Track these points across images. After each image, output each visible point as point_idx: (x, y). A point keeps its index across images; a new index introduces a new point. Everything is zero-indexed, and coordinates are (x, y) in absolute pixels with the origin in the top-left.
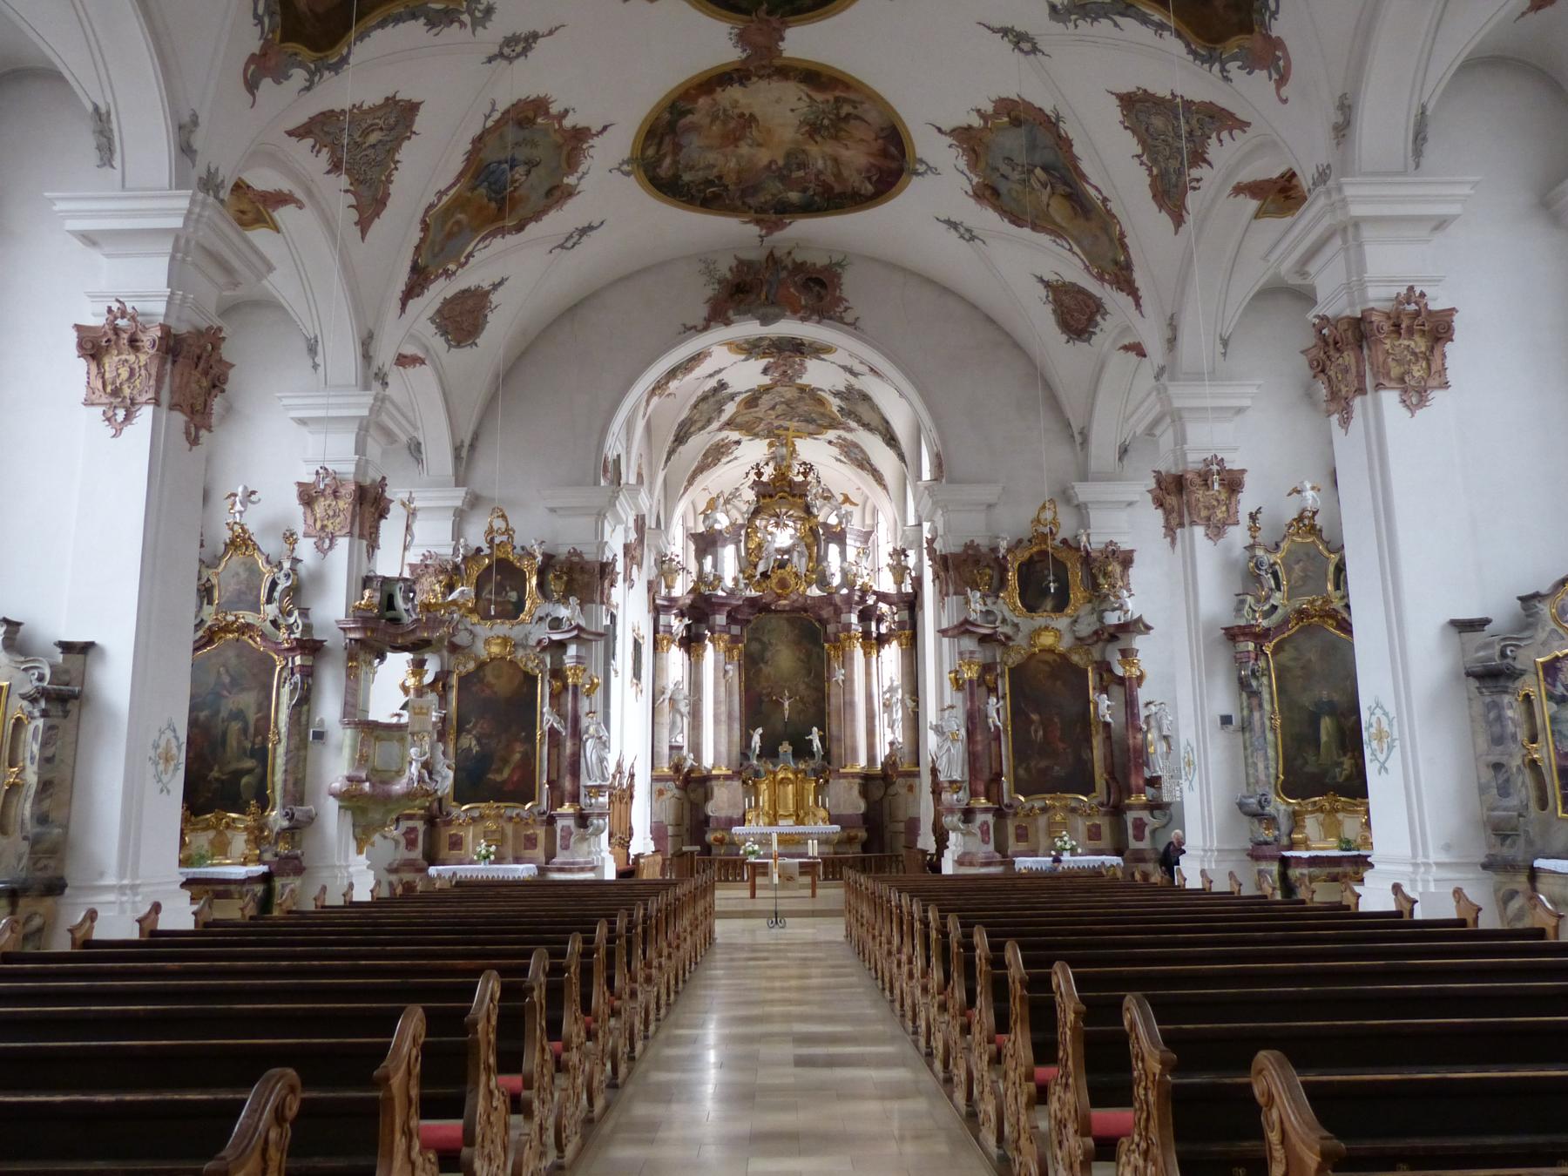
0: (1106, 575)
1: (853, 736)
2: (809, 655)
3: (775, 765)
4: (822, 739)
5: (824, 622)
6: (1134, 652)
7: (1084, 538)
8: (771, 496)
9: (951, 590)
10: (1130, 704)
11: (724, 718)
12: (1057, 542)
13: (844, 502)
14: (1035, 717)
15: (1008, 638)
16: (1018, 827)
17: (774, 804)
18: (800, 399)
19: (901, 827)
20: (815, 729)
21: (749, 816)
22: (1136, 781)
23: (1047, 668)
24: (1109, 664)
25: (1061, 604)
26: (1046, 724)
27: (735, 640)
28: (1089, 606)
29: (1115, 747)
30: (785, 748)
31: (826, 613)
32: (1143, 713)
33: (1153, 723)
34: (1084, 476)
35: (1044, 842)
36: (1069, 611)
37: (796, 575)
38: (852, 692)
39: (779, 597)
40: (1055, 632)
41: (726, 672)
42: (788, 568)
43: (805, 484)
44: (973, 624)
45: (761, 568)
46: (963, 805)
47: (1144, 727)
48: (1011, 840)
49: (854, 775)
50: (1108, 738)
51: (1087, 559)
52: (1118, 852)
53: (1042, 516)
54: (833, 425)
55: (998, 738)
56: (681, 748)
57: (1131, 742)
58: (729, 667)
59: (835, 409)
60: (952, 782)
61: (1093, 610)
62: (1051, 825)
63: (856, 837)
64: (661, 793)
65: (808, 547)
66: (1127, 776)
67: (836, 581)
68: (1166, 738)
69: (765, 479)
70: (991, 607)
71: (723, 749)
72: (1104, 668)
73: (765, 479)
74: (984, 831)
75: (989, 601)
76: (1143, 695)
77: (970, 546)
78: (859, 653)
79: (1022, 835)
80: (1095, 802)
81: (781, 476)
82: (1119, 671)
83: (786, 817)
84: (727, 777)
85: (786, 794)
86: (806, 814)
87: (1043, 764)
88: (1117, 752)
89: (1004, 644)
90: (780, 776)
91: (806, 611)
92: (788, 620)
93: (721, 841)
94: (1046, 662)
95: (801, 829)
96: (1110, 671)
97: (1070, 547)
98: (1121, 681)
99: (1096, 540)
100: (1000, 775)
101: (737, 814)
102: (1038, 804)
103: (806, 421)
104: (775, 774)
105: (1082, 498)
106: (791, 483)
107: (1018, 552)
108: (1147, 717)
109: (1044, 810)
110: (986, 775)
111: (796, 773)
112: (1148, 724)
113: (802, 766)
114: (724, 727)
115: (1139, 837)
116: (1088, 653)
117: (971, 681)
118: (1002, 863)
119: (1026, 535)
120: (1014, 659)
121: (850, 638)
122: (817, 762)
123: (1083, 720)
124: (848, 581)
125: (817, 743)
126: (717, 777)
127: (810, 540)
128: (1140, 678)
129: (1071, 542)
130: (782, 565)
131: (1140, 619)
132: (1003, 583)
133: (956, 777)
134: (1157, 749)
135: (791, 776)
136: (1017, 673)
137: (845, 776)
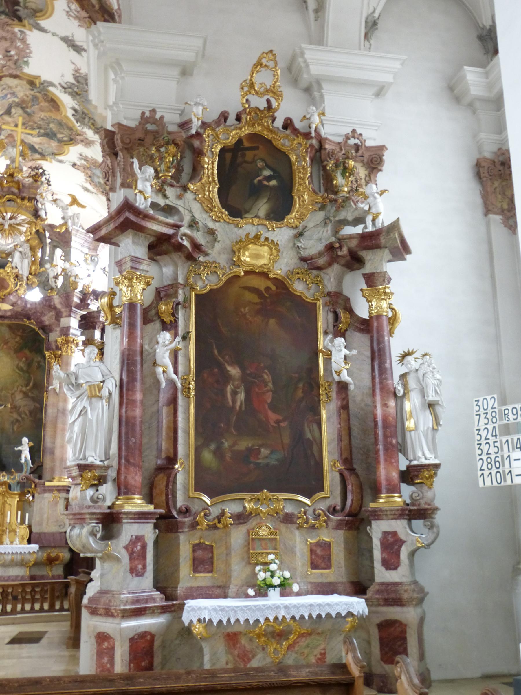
0: (346, 171)
2: (29, 365)
4: (32, 450)
5: (46, 329)
6: (386, 279)
7: (316, 120)
9: (119, 180)
10: (378, 355)
12: (279, 123)
13: (71, 204)
14: (234, 371)
15: (197, 247)
16: (196, 547)
18: (35, 99)
20: (25, 440)
22: (385, 473)
23: (255, 299)
24: (347, 300)
25: (280, 211)
26: (250, 383)
28: (321, 215)
29: (354, 422)
31: (48, 319)
32: (398, 370)
33: (412, 383)
34: (319, 40)
35: (238, 571)
36: (291, 218)
37: (17, 276)
40: (270, 248)
44: (137, 212)
46: (103, 507)
47: (400, 391)
48: (185, 569)
50: (345, 407)
51: (319, 153)
52: (359, 589)
53: (258, 79)
54: (72, 141)
55: (173, 402)
57: (379, 412)
59: (70, 113)
60: (83, 468)
61: (326, 221)
62: (251, 542)
63: (57, 558)
65: (33, 249)
66: (372, 467)
68: (431, 406)
70: (172, 200)
72: (339, 303)
74: (136, 554)
75: (170, 192)
76: (396, 345)
77: (149, 119)
79: (203, 560)
80: (323, 506)
82: (362, 310)
87: (243, 445)
88: (355, 432)
89: (190, 257)
91: (29, 319)
92: (10, 327)
94: (255, 291)
96: (350, 310)
97: (296, 131)
98: (366, 326)
99: (333, 131)
100: (172, 459)
102: (232, 509)
103: (46, 135)
105: (314, 70)
107: (220, 130)
108: (403, 377)
109: (241, 518)
110: (152, 460)
112: (405, 386)
115: (391, 564)
116: (319, 282)
117: (132, 306)
118: (164, 610)
119: (234, 107)
120: (205, 283)
121: (67, 342)
123: (307, 384)
127: (36, 242)
128: (393, 320)
129: (298, 124)
131: (395, 226)
132: (196, 170)
133: (94, 458)
134: (416, 421)
136: (209, 305)
137: (51, 490)
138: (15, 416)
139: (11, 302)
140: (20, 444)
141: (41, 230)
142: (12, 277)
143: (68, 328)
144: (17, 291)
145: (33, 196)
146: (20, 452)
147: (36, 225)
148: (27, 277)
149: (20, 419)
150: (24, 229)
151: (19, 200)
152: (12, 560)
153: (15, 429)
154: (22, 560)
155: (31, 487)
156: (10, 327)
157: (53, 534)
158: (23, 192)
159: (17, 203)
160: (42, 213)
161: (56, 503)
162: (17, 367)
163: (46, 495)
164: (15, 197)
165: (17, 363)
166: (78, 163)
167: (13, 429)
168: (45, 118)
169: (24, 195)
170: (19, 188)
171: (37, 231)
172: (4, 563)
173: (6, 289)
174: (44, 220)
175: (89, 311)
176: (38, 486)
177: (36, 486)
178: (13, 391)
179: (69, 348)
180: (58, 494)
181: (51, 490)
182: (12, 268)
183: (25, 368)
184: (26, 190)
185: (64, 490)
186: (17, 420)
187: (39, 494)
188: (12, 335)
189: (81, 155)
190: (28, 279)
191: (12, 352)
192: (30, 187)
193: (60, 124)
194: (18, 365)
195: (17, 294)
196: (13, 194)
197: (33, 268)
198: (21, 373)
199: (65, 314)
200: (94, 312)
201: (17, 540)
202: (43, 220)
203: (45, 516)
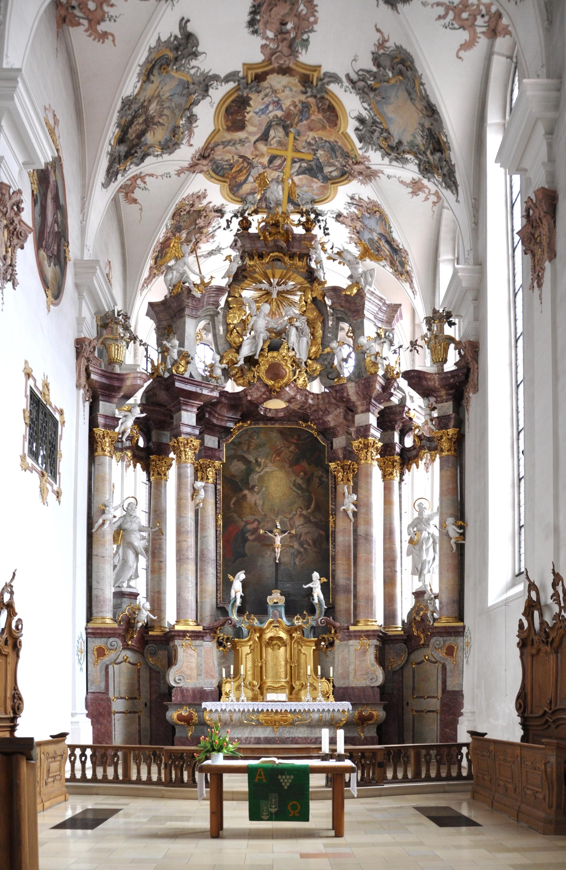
1: (369, 582)
3: (261, 622)
8: (261, 256)
11: (191, 554)
17: (260, 672)
19: (435, 704)
21: (226, 688)
27: (205, 453)
30: (276, 598)
37: (296, 363)
38: (369, 523)
39: (271, 393)
41: (195, 491)
42: (283, 351)
43: (309, 238)
45: (245, 351)
49: (369, 634)
56: (134, 596)
58: (199, 484)
64: (101, 652)
65: (310, 323)
67: (348, 369)
71: (190, 597)
73: (253, 230)
78: (376, 473)
81: (274, 226)
83: (274, 690)
84: (196, 636)
85: (276, 658)
86: (303, 686)
90: (269, 635)
93: (188, 720)
95: (294, 706)
101: (210, 685)
104: (262, 631)
111: (289, 632)
113: (298, 622)
114: (191, 567)
121: (366, 446)
122: (319, 619)
124: (364, 377)
125: (318, 593)
126: (183, 634)
127: (313, 314)
135: (283, 635)
137: (358, 635)
139: (287, 397)
140: (311, 580)
141: (320, 298)
142: (289, 362)
143: (367, 428)
144: (295, 380)
145: (305, 251)
146: (311, 589)
147: (312, 291)
148: (305, 363)
150: (296, 298)
151: (286, 259)
152: (320, 720)
154: (332, 720)
155: (331, 633)
157: (363, 689)
158: (293, 248)
159: (285, 263)
160: (320, 275)
161: (365, 652)
163: (351, 642)
164: (282, 255)
168: (313, 142)
169: (295, 250)
170: (287, 241)
171: (314, 300)
172: (310, 722)
175: (388, 404)
176: (338, 631)
177: (335, 632)
179: (369, 454)
180: (366, 641)
181: (358, 635)
184: (296, 244)
185: (374, 635)
187: (341, 641)
190: (306, 365)
193: (333, 149)
195: (296, 386)
196: (279, 249)
197: (314, 349)
199: (360, 409)
200: (396, 406)
201: (320, 697)
202: (322, 283)
203: (352, 667)
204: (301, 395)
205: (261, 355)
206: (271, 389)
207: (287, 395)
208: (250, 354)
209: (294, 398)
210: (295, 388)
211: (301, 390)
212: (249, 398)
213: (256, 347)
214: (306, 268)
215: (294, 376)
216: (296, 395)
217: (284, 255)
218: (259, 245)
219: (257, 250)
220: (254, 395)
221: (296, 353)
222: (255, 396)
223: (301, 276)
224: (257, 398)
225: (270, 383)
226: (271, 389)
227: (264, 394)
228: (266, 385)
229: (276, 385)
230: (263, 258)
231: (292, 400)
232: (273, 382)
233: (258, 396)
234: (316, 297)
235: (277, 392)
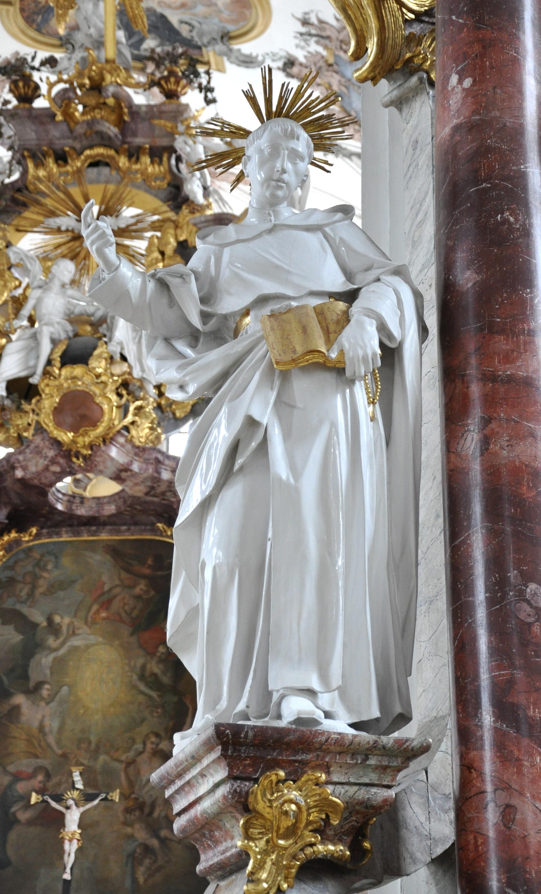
8: (62, 158)
39: (68, 459)
69: (40, 103)
92: (115, 551)
106: (127, 116)
130: (75, 355)
138: (140, 834)
139: (111, 469)
142: (111, 387)
144: (126, 428)
145: (164, 142)
147: (177, 226)
149: (154, 843)
151: (123, 161)
153: (141, 880)
156: (115, 551)
158: (135, 135)
159: (118, 169)
162: (142, 677)
164: (112, 152)
165: (141, 661)
166: (300, 56)
167: (134, 880)
169: (138, 140)
170: (120, 123)
173: (94, 424)
174: (202, 208)
178: (131, 754)
182: (111, 359)
183: (166, 680)
184: (142, 127)
186: (147, 849)
188: (124, 575)
189: (305, 22)
191: (125, 631)
192: (153, 112)
194: (143, 667)
195: (130, 441)
196: (105, 141)
198: (154, 694)
202: (195, 208)
204: (146, 461)
205: (46, 373)
206: (70, 451)
207: (109, 464)
208: (23, 374)
209: (126, 469)
210: (129, 447)
211: (144, 449)
212: (19, 474)
213: (38, 357)
214: (169, 177)
215: (125, 415)
216: (131, 463)
217: (117, 152)
218: (55, 132)
219: (50, 145)
220: (32, 467)
221: (130, 367)
222: (33, 469)
223: (156, 196)
224: (38, 474)
225: (67, 437)
226: (70, 451)
227: (53, 461)
228: (57, 443)
229: (80, 440)
230: (66, 162)
231: (124, 475)
232: (71, 435)
233: (40, 468)
234: (186, 241)
235: (85, 458)
